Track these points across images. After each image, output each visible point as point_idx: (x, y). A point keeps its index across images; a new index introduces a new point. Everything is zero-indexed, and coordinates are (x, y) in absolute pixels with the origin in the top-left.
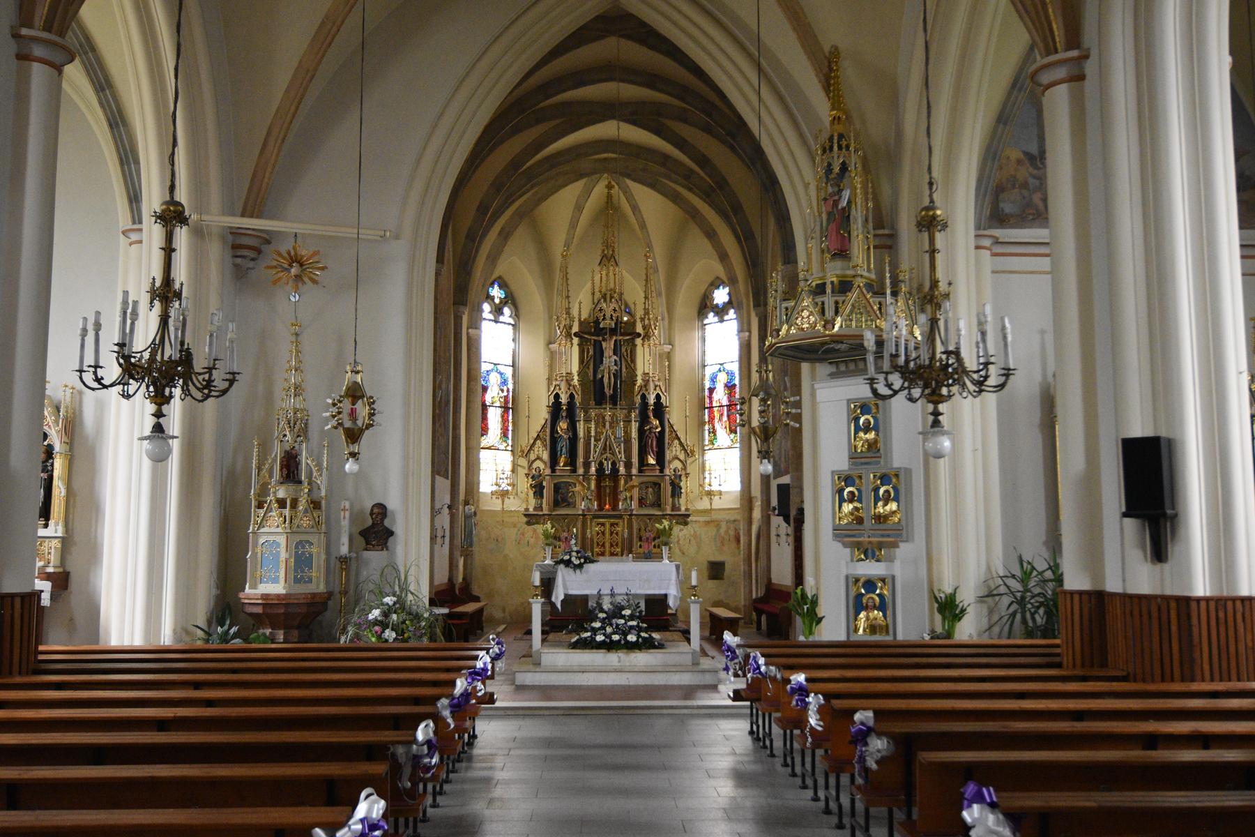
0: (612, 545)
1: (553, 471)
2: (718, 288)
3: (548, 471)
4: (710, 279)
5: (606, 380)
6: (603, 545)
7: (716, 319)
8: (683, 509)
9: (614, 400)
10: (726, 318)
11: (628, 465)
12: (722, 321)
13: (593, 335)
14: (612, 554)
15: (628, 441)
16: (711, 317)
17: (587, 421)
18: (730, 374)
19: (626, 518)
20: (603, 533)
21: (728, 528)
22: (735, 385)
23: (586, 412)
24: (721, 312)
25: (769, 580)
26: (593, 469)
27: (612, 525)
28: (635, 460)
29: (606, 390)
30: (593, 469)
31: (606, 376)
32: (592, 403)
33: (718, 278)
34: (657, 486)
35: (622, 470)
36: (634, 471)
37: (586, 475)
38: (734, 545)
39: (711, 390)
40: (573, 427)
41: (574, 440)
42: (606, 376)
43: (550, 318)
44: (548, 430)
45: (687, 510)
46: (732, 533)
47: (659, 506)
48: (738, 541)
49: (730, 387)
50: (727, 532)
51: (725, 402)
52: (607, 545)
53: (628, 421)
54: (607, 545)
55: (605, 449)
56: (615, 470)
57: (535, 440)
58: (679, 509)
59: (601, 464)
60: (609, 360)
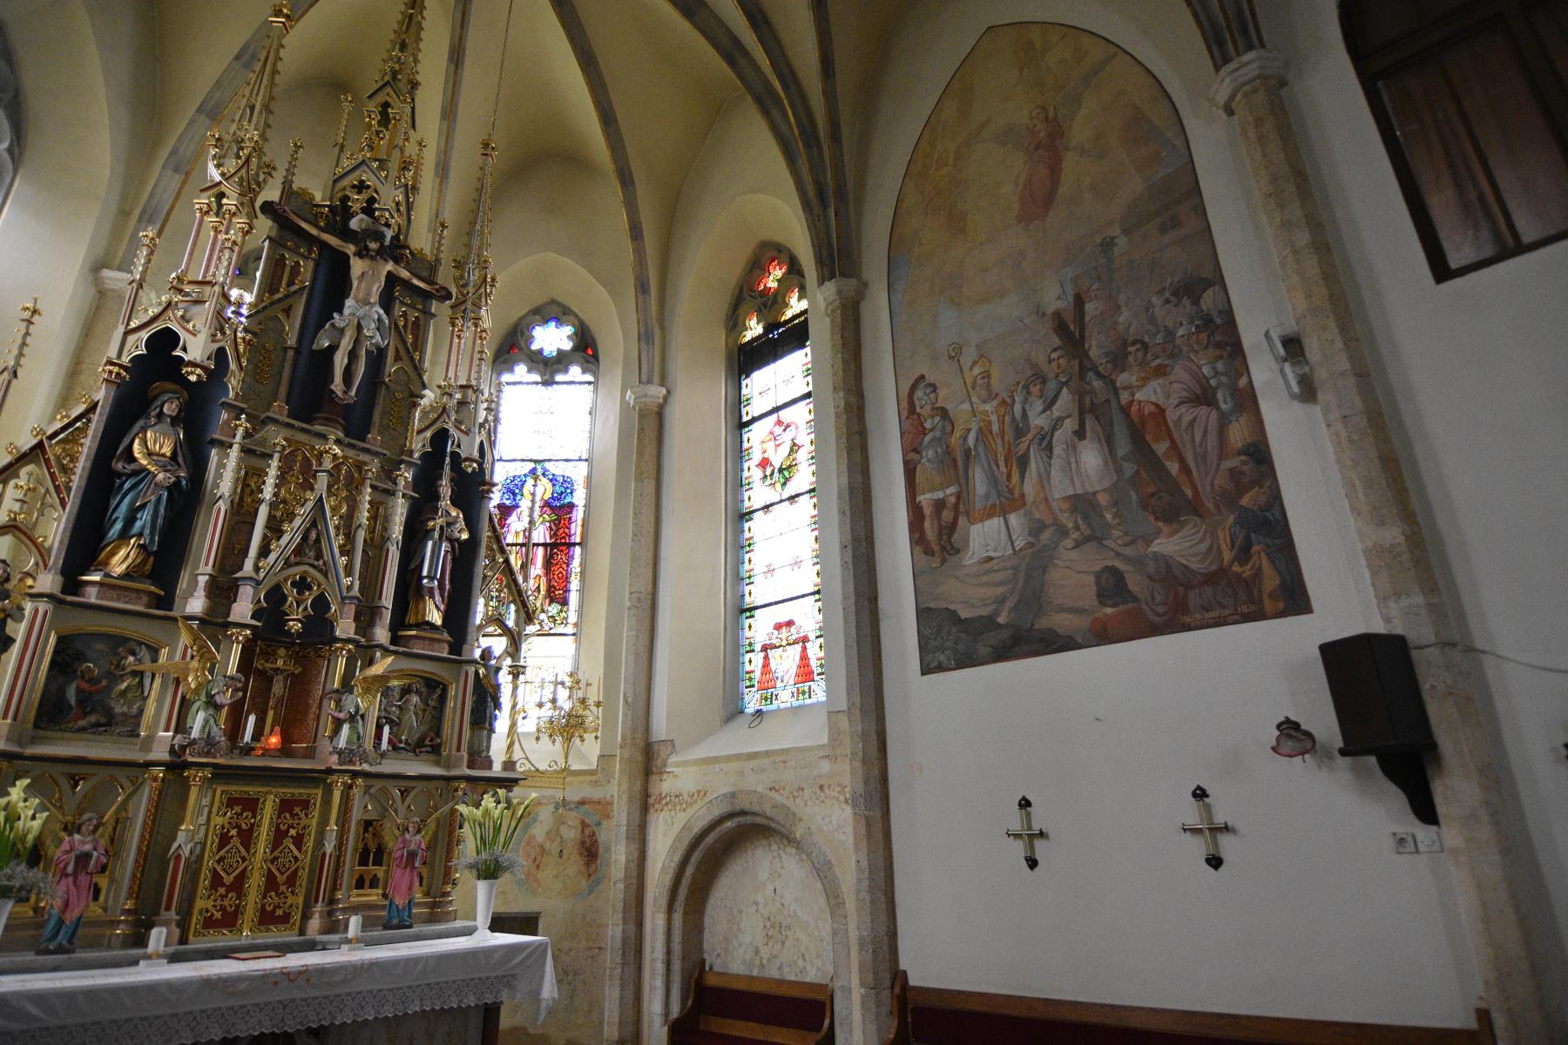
0: (271, 883)
1: (72, 584)
2: (545, 322)
3: (48, 582)
4: (539, 299)
5: (340, 360)
6: (238, 885)
7: (537, 377)
8: (497, 767)
9: (356, 424)
10: (559, 378)
11: (366, 616)
12: (548, 382)
13: (316, 248)
14: (267, 918)
15: (377, 545)
16: (521, 370)
17: (254, 454)
18: (566, 485)
19: (339, 783)
20: (247, 837)
21: (560, 822)
22: (571, 506)
23: (258, 422)
24: (549, 368)
25: (899, 977)
26: (242, 609)
27: (286, 806)
28: (388, 599)
29: (337, 385)
30: (242, 609)
31: (346, 343)
32: (279, 410)
33: (553, 302)
34: (434, 688)
35: (345, 627)
36: (382, 634)
37: (215, 623)
38: (574, 864)
39: (506, 511)
40: (194, 453)
41: (186, 500)
42: (346, 343)
43: (124, 213)
44: (88, 445)
45: (509, 765)
46: (571, 834)
47: (436, 750)
48: (590, 852)
49: (559, 510)
50: (553, 833)
51: (541, 535)
52: (255, 882)
53: (385, 493)
54: (255, 882)
55: (298, 551)
56: (319, 624)
57: (23, 459)
58: (488, 764)
59: (276, 596)
60: (362, 309)
